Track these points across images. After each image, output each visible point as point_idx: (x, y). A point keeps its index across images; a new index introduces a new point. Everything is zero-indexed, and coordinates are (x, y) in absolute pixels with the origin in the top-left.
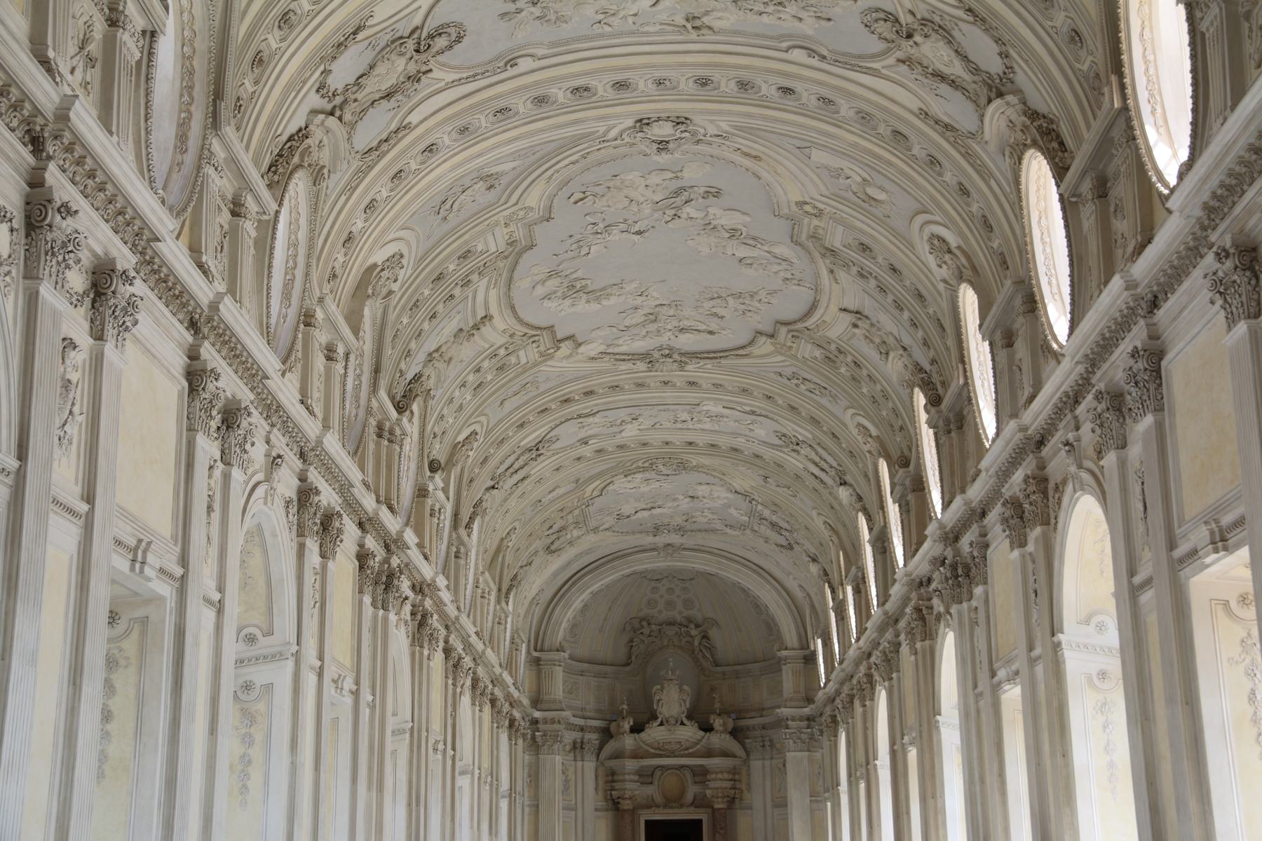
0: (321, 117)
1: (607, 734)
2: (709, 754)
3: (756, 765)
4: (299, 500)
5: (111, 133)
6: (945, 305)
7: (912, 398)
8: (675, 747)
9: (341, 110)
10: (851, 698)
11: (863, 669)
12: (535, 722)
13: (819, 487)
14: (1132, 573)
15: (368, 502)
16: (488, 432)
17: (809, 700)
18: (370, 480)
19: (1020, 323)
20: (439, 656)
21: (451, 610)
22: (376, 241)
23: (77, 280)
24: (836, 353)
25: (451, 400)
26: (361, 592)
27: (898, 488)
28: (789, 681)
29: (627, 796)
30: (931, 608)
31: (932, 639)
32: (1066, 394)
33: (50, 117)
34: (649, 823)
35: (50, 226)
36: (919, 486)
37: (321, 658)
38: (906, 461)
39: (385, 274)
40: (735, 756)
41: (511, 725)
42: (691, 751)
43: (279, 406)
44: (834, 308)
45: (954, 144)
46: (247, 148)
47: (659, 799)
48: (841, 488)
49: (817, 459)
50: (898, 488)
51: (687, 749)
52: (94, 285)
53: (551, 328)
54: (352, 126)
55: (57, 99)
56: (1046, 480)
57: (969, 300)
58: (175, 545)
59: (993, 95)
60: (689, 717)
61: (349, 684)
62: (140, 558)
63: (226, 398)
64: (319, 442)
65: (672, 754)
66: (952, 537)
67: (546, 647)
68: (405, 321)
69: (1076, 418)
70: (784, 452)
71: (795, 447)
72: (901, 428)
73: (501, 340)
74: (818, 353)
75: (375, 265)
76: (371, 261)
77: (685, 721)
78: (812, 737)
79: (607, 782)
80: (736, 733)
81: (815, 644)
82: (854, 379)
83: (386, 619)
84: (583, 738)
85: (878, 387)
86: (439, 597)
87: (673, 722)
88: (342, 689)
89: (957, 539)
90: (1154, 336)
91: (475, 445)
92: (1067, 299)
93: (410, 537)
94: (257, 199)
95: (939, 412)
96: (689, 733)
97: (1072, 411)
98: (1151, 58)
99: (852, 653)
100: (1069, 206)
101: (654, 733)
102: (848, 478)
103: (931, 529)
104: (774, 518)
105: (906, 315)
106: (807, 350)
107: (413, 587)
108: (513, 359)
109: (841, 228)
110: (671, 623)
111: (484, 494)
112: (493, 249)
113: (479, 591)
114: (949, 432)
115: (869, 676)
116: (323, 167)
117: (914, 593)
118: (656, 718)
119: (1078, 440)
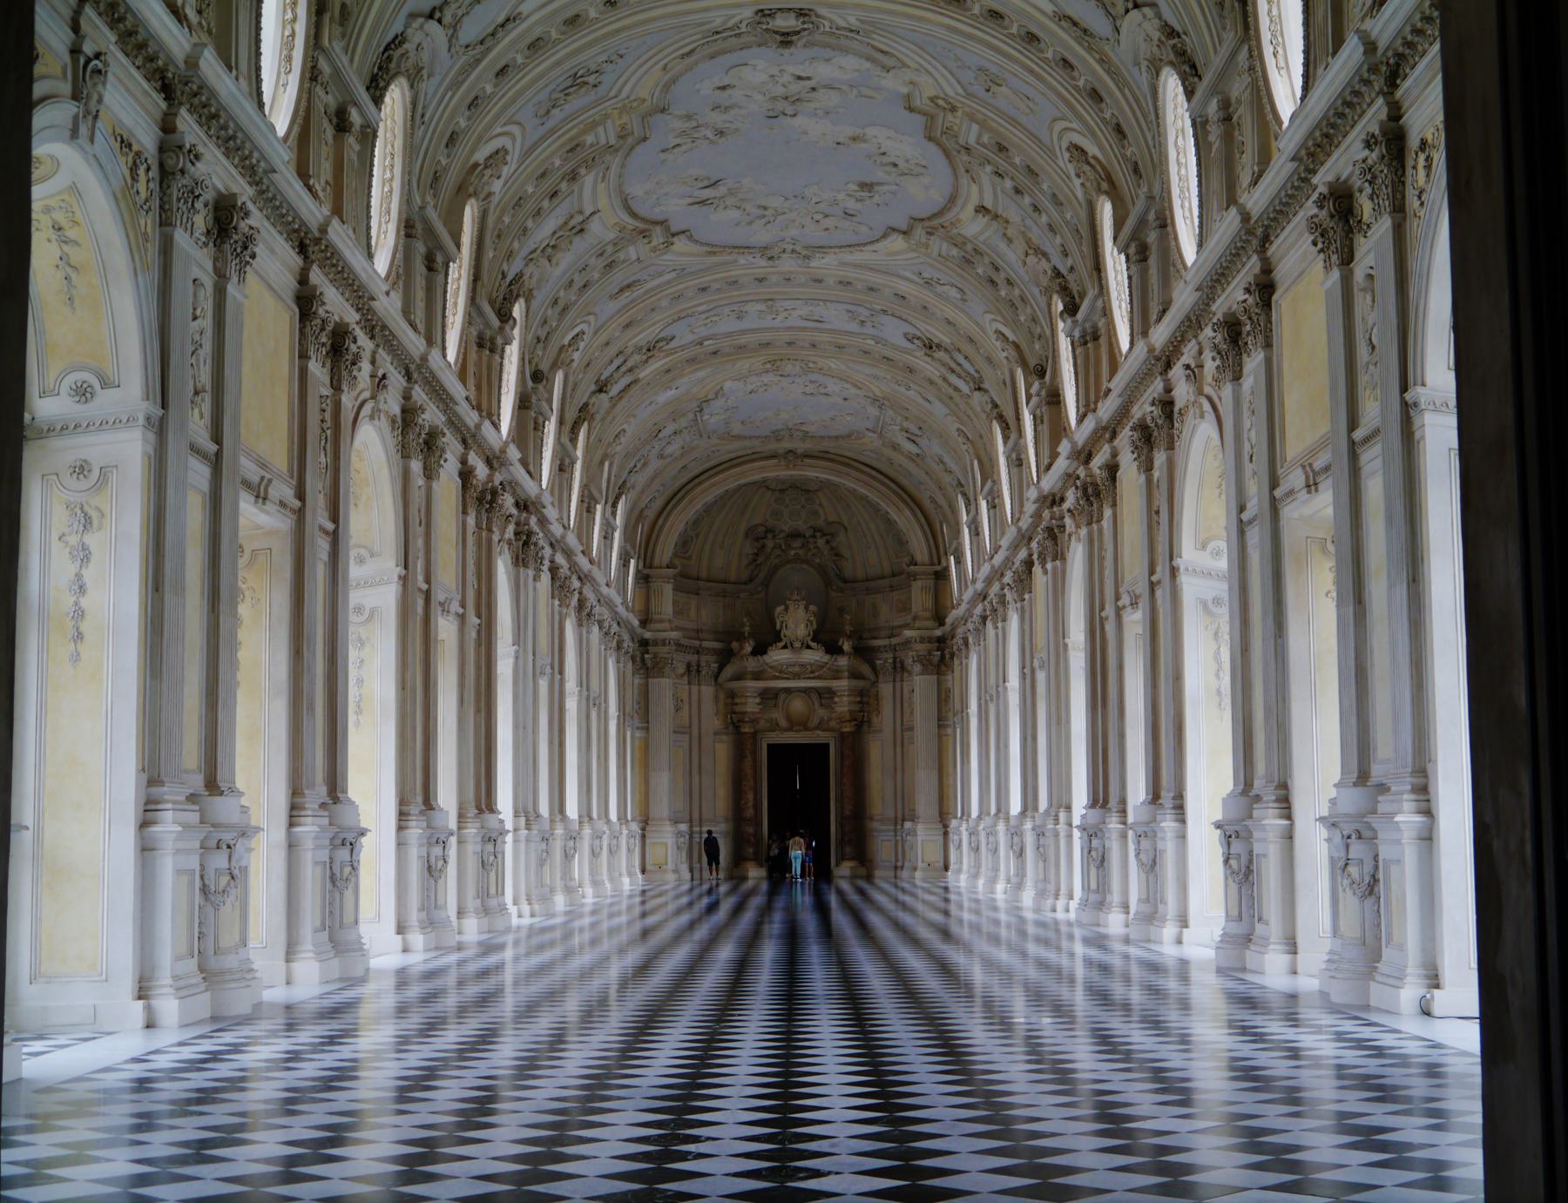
0: (421, 20)
1: (726, 656)
2: (836, 675)
3: (886, 689)
4: (404, 420)
5: (230, 69)
6: (1083, 214)
7: (1049, 305)
8: (797, 669)
9: (441, 11)
10: (984, 618)
11: (996, 588)
12: (644, 643)
13: (954, 394)
14: (1242, 509)
15: (471, 417)
16: (596, 333)
17: (940, 620)
18: (473, 395)
19: (1152, 237)
20: (546, 577)
21: (556, 529)
22: (480, 138)
23: (201, 221)
24: (973, 253)
25: (556, 302)
26: (465, 512)
27: (1034, 400)
28: (920, 597)
30: (1064, 527)
31: (1064, 559)
32: (1188, 318)
33: (182, 65)
34: (770, 746)
35: (182, 171)
36: (1054, 398)
37: (428, 581)
38: (1042, 370)
39: (488, 172)
41: (619, 647)
43: (384, 327)
44: (970, 209)
45: (1090, 49)
46: (352, 60)
47: (783, 723)
48: (977, 393)
49: (953, 365)
50: (1034, 400)
51: (812, 672)
52: (217, 220)
53: (662, 223)
54: (455, 26)
55: (187, 47)
56: (1171, 403)
57: (1106, 211)
58: (292, 477)
59: (1130, 5)
60: (813, 640)
61: (455, 607)
62: (262, 494)
63: (336, 323)
64: (424, 358)
65: (796, 676)
66: (1084, 455)
67: (656, 562)
68: (507, 219)
69: (1199, 343)
70: (916, 357)
71: (928, 351)
72: (1040, 336)
73: (611, 236)
74: (955, 252)
75: (476, 165)
76: (472, 161)
78: (943, 657)
79: (726, 704)
80: (864, 652)
81: (948, 560)
82: (992, 282)
83: (490, 541)
84: (699, 661)
85: (1017, 292)
86: (542, 513)
87: (797, 645)
88: (448, 612)
89: (1089, 457)
90: (1267, 270)
91: (582, 345)
92: (1196, 221)
93: (514, 453)
94: (362, 113)
95: (1075, 322)
96: (815, 656)
97: (1196, 337)
99: (986, 569)
100: (1200, 126)
101: (777, 656)
102: (985, 386)
103: (1064, 448)
104: (906, 424)
105: (1044, 219)
106: (938, 245)
107: (517, 505)
108: (621, 255)
109: (975, 127)
110: (795, 535)
111: (590, 397)
112: (603, 141)
113: (585, 505)
114: (1085, 343)
115: (1002, 600)
116: (422, 68)
117: (1047, 511)
118: (780, 640)
119: (1201, 366)
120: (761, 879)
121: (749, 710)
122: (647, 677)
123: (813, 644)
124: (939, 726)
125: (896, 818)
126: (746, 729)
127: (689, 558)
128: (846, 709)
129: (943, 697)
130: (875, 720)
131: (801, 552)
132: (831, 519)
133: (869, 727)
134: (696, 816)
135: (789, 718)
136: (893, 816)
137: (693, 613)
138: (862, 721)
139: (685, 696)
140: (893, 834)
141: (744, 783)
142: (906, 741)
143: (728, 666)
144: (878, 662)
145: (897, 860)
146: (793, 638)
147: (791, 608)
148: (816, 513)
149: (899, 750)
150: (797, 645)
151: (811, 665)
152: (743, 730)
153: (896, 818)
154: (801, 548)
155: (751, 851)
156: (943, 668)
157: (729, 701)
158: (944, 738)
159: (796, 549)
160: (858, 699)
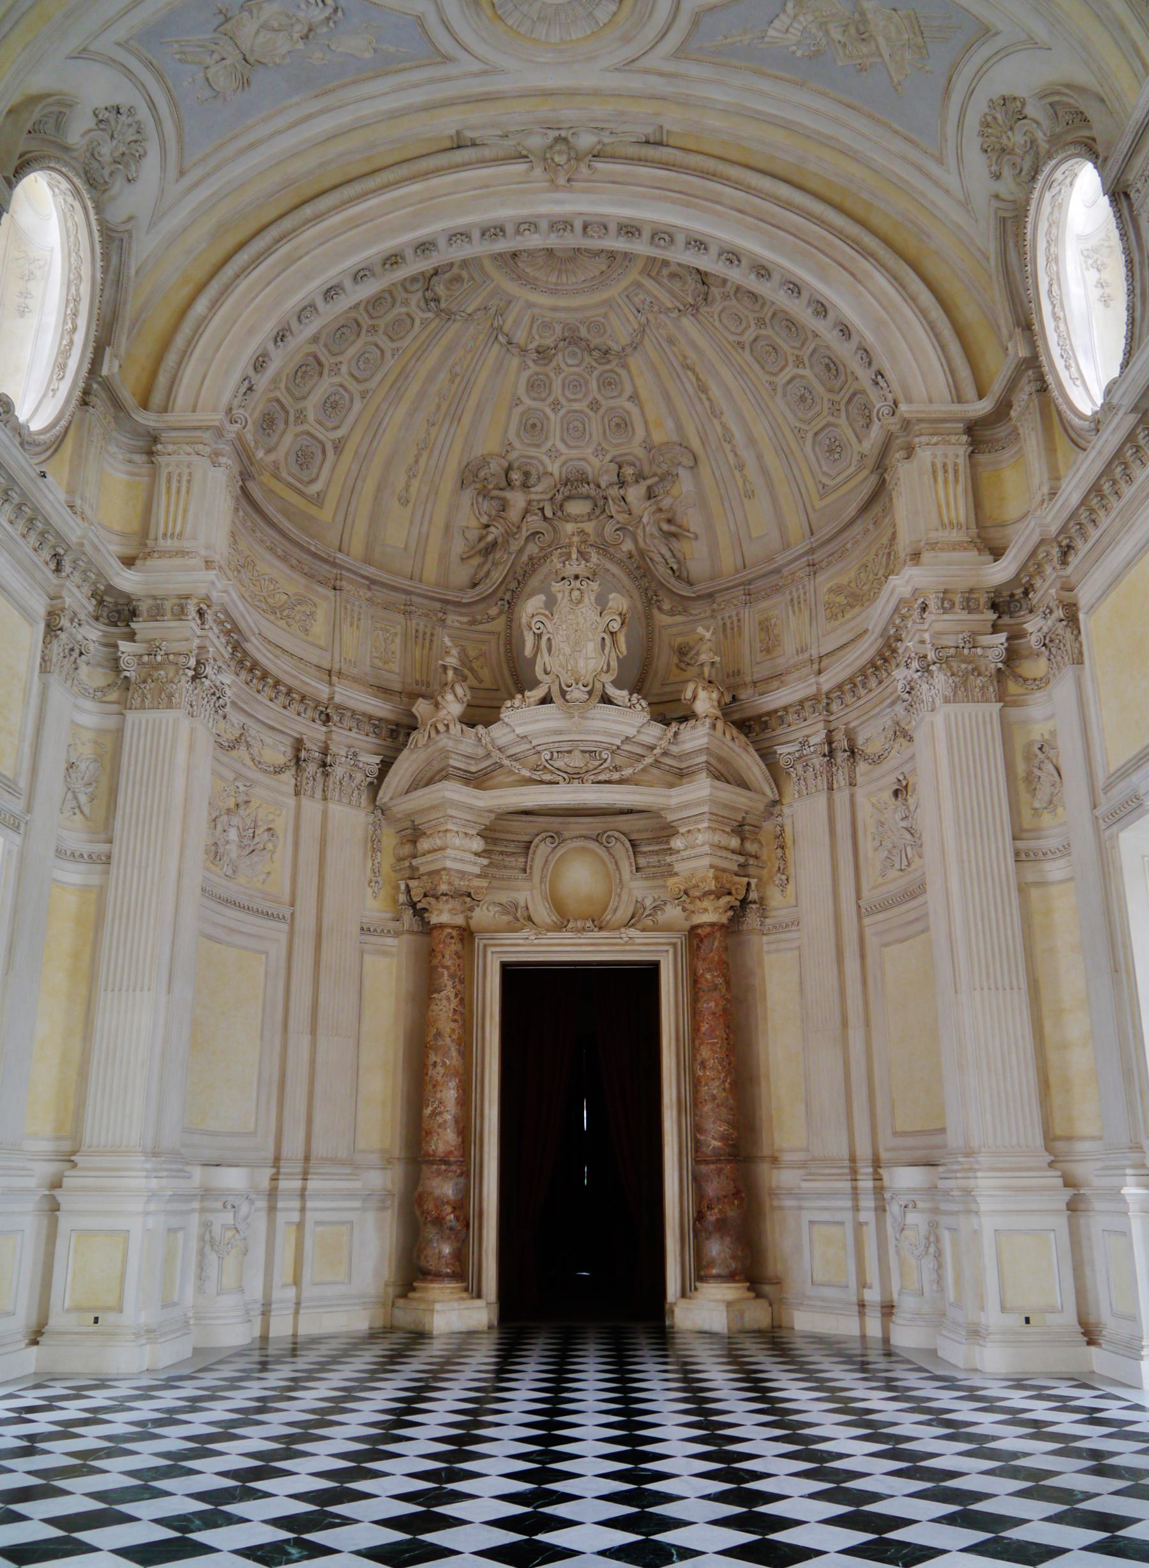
8: (577, 761)
29: (444, 888)
34: (513, 974)
40: (743, 784)
42: (627, 772)
60: (618, 684)
65: (575, 776)
77: (612, 691)
78: (1012, 656)
87: (577, 694)
98: (1061, 314)
118: (535, 683)
120: (471, 1334)
121: (449, 864)
122: (125, 705)
123: (619, 695)
124: (1018, 857)
125: (853, 1159)
126: (443, 915)
127: (318, 500)
128: (706, 861)
129: (1021, 768)
130: (775, 898)
131: (589, 527)
132: (658, 437)
133: (763, 913)
134: (293, 1146)
135: (557, 905)
136: (845, 1154)
137: (319, 628)
138: (744, 902)
139: (283, 823)
140: (849, 1204)
141: (433, 1058)
142: (872, 942)
143: (406, 752)
144: (782, 750)
145: (863, 1284)
146: (565, 678)
147: (563, 603)
148: (623, 425)
149: (852, 966)
150: (577, 694)
151: (615, 750)
152: (434, 919)
153: (853, 1159)
154: (589, 517)
155: (447, 1250)
156: (1013, 687)
157: (407, 849)
158: (1034, 893)
159: (575, 519)
160: (734, 842)
